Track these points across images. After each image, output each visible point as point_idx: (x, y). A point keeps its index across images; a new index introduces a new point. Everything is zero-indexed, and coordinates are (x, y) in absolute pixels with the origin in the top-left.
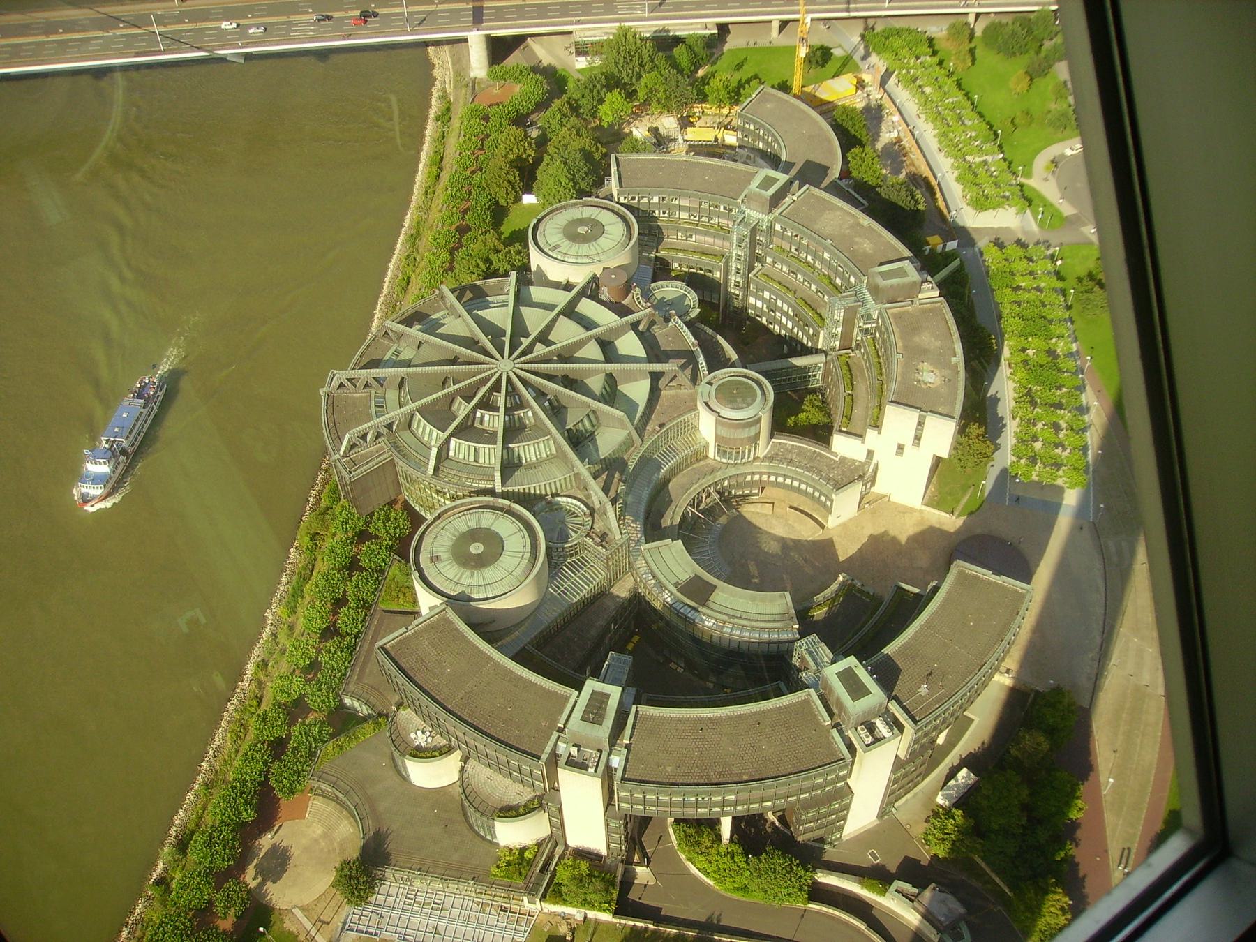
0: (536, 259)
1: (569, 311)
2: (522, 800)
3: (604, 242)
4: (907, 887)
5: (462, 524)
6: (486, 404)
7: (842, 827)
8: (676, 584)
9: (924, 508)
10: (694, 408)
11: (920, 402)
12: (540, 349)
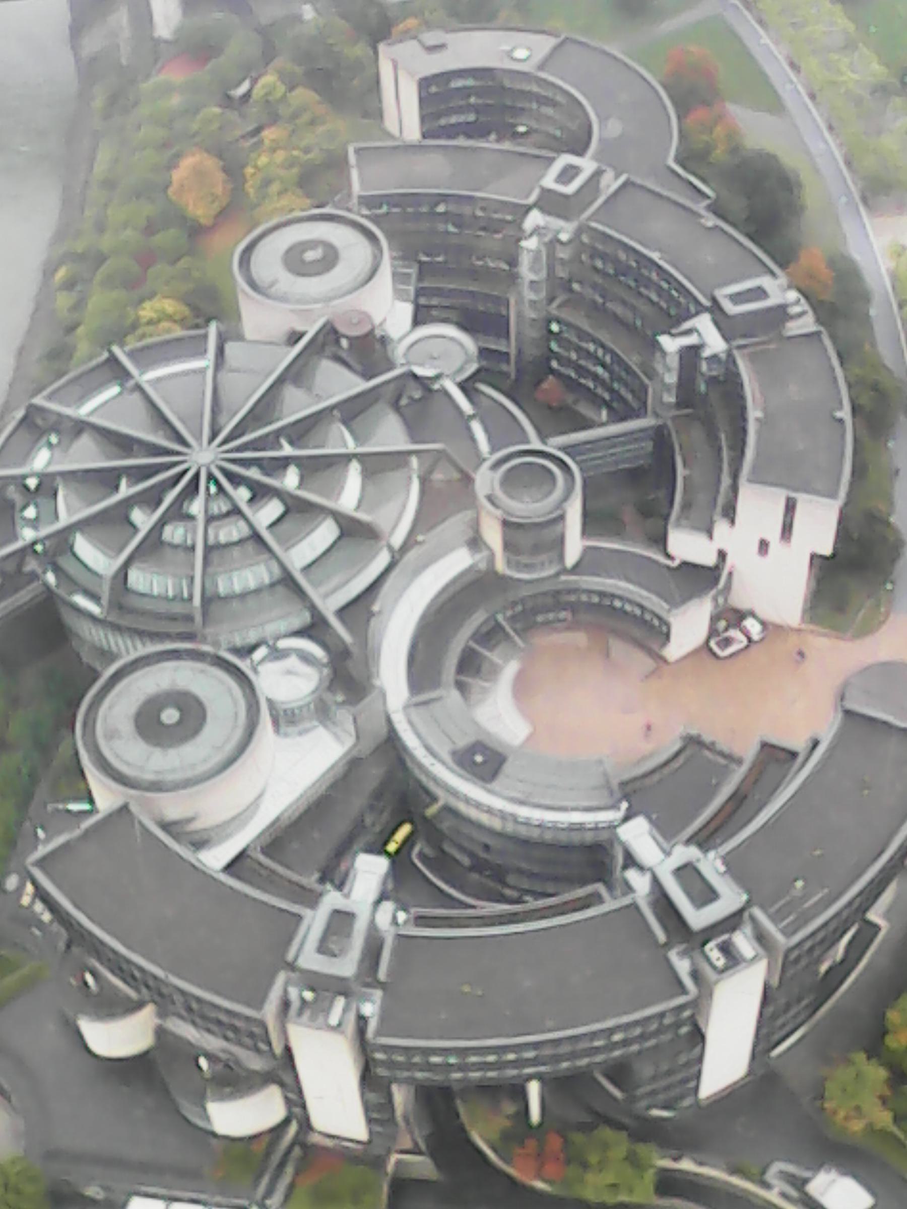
6: (178, 513)
7: (696, 1089)
8: (454, 753)
9: (803, 626)
11: (791, 476)
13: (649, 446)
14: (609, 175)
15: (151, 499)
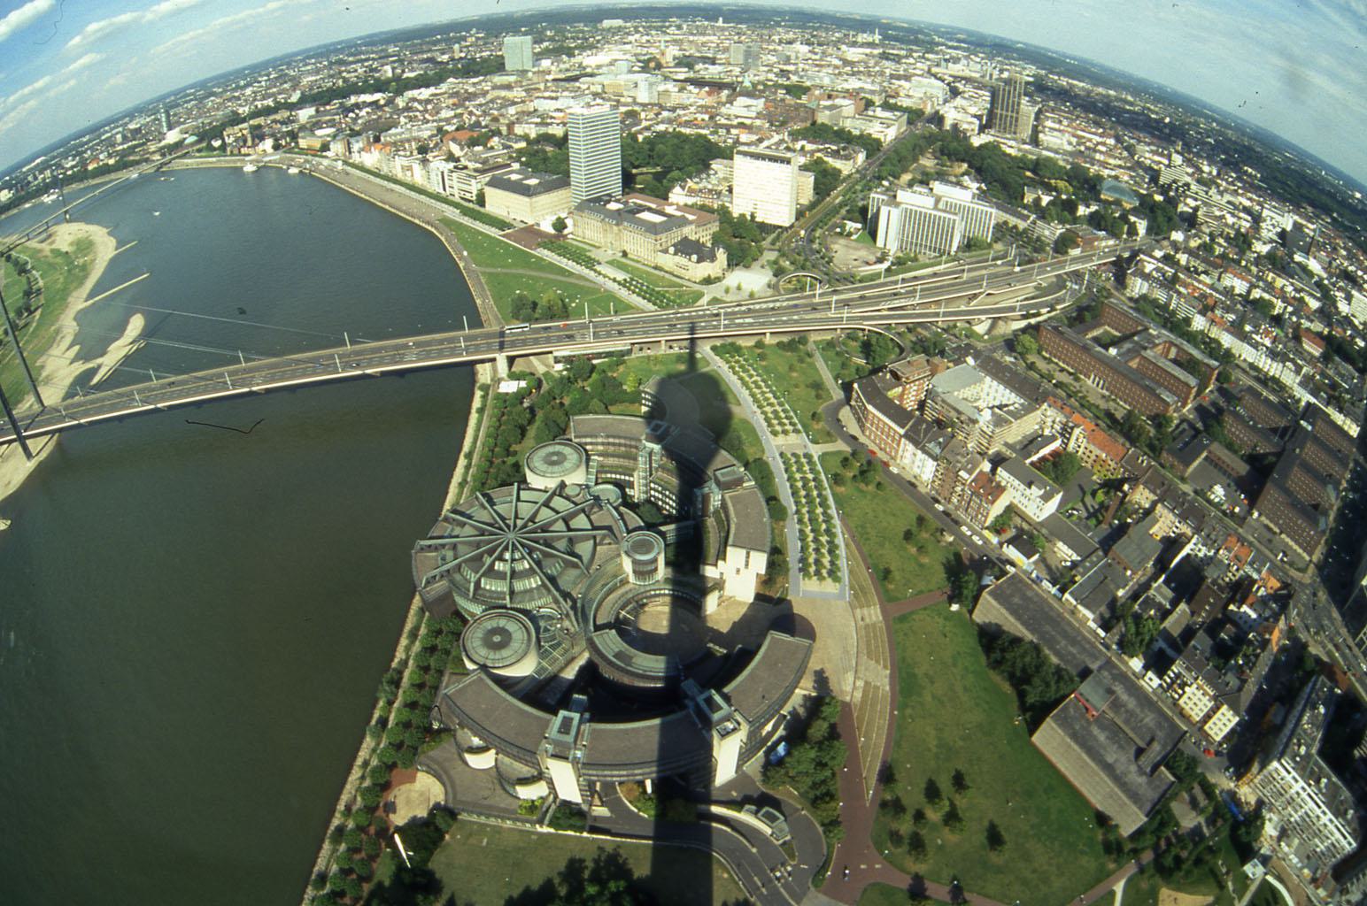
0: (530, 477)
1: (546, 504)
2: (529, 775)
3: (567, 465)
4: (754, 808)
5: (489, 625)
6: (500, 558)
10: (619, 555)
12: (531, 526)
13: (692, 531)
14: (673, 428)
15: (491, 552)
